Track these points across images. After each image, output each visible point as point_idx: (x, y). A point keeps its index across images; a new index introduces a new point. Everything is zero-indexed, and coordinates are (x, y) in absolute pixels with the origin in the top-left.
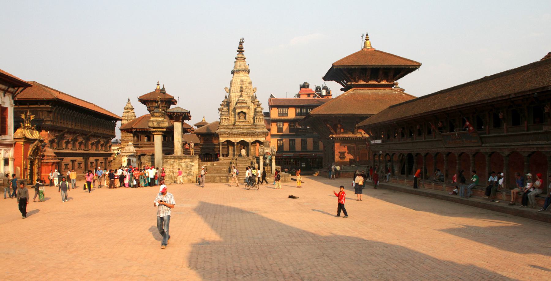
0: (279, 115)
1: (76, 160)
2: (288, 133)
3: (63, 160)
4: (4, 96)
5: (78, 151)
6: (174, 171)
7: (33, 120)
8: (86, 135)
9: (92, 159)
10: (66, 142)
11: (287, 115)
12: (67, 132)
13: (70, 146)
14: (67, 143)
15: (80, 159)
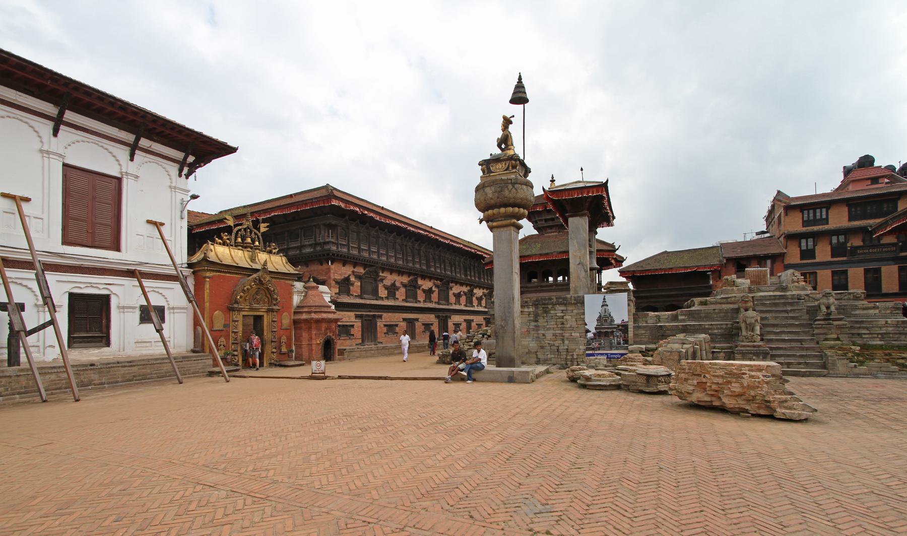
0: (805, 223)
1: (417, 320)
2: (828, 258)
3: (380, 317)
4: (132, 159)
5: (421, 305)
6: (567, 335)
7: (263, 234)
8: (441, 280)
9: (456, 318)
10: (386, 288)
11: (826, 221)
12: (392, 272)
13: (401, 293)
14: (392, 290)
15: (431, 318)
